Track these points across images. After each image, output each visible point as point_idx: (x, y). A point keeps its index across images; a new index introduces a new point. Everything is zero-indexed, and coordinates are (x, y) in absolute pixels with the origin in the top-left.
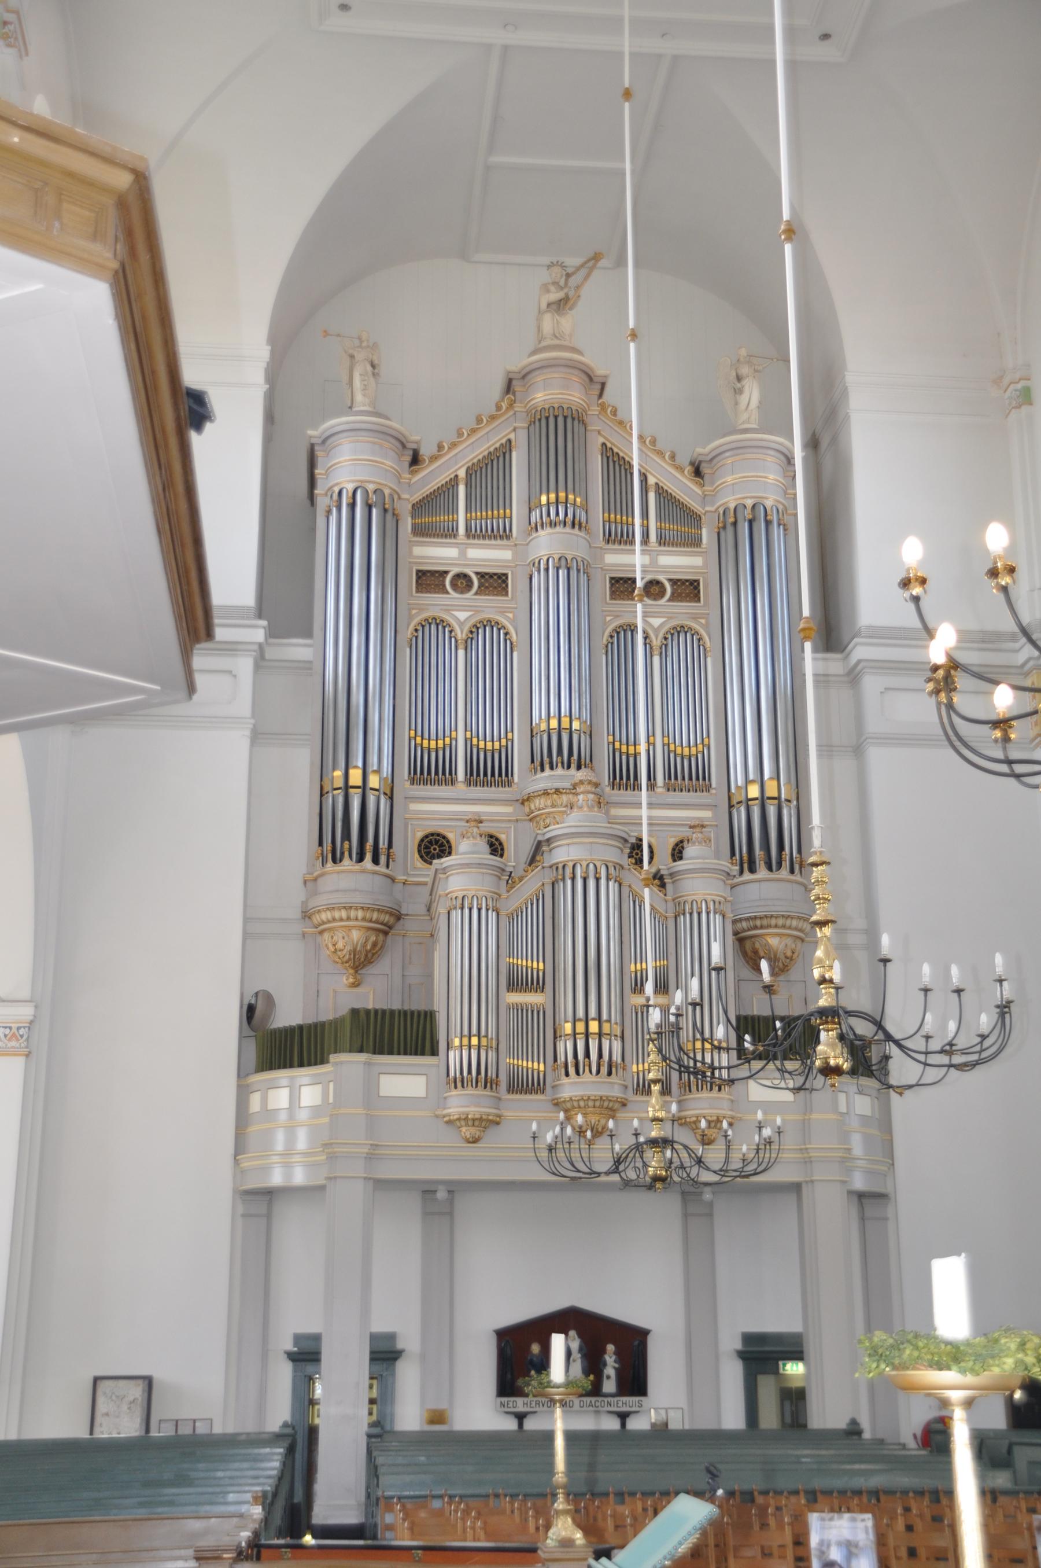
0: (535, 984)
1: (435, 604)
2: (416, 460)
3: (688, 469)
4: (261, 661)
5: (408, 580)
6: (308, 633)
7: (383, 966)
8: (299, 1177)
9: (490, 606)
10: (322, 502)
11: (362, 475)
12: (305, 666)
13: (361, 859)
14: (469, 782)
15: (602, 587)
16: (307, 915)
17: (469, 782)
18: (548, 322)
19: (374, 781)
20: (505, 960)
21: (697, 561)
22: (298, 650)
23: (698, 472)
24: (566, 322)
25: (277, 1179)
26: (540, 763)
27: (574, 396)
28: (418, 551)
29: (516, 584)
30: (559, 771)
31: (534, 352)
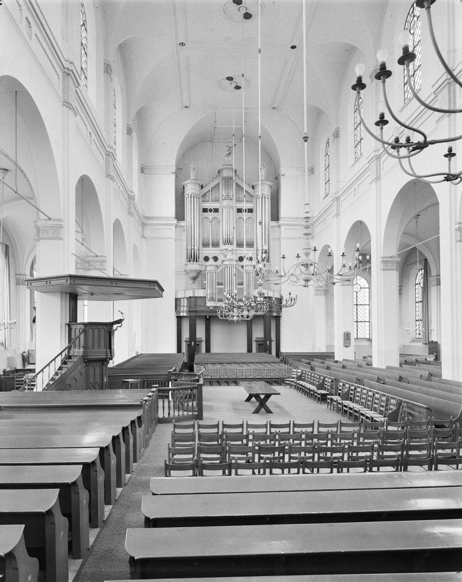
0: (222, 284)
2: (202, 187)
3: (251, 187)
4: (176, 226)
5: (201, 210)
6: (184, 220)
7: (198, 279)
8: (185, 314)
9: (216, 214)
10: (186, 196)
11: (193, 191)
12: (184, 227)
13: (194, 261)
15: (235, 211)
16: (185, 271)
18: (226, 158)
19: (196, 248)
20: (217, 281)
21: (253, 205)
22: (182, 223)
23: (253, 188)
24: (230, 159)
25: (182, 314)
26: (225, 244)
27: (231, 174)
28: (203, 205)
29: (220, 210)
30: (227, 245)
31: (223, 166)
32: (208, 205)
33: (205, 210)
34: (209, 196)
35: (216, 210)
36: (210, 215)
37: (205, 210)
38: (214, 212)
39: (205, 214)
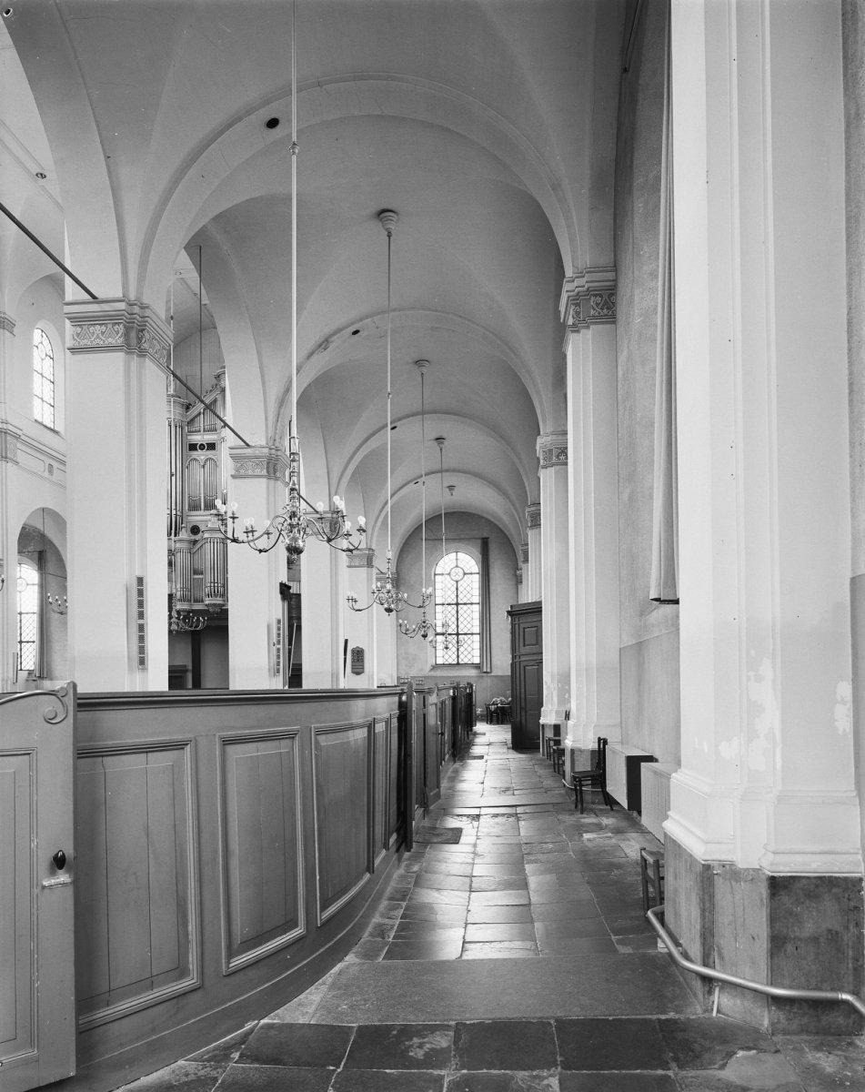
1: (195, 454)
5: (186, 447)
9: (210, 454)
14: (204, 510)
17: (204, 510)
28: (189, 438)
32: (197, 438)
33: (193, 447)
34: (200, 423)
35: (212, 446)
36: (201, 455)
37: (193, 447)
38: (208, 449)
39: (195, 453)
